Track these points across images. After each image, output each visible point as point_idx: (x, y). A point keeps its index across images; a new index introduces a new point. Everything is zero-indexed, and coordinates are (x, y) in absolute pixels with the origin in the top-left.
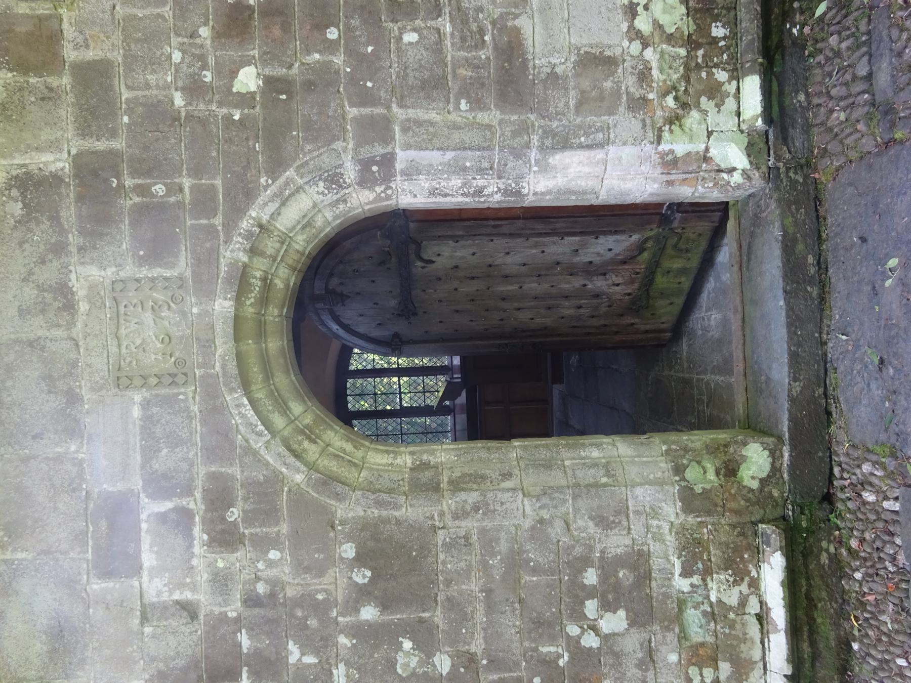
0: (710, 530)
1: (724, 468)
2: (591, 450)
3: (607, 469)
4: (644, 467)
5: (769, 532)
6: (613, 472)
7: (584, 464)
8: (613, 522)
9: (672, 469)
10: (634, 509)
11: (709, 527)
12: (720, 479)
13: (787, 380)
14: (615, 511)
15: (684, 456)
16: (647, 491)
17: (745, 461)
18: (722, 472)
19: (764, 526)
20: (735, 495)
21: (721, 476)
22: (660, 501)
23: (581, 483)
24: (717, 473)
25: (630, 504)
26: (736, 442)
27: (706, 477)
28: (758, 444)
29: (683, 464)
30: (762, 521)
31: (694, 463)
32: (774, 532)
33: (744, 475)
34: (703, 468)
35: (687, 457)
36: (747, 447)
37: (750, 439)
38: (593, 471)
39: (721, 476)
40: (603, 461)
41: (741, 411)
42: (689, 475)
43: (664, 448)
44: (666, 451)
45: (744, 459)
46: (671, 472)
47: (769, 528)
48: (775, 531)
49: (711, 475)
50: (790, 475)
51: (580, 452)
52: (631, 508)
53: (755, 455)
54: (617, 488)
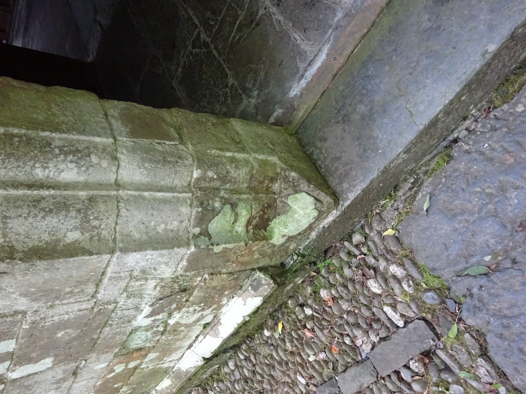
0: (205, 279)
1: (259, 217)
2: (62, 166)
3: (86, 216)
4: (155, 213)
5: (263, 282)
6: (96, 223)
7: (37, 202)
8: (71, 292)
9: (196, 217)
10: (114, 275)
11: (206, 276)
12: (248, 232)
13: (400, 150)
14: (78, 282)
15: (218, 189)
16: (146, 256)
17: (285, 212)
18: (254, 222)
19: (262, 275)
20: (254, 251)
21: (251, 227)
22: (159, 263)
23: (19, 247)
24: (249, 223)
25: (109, 270)
26: (286, 179)
27: (233, 227)
28: (312, 200)
29: (213, 209)
30: (260, 269)
31: (228, 208)
32: (269, 284)
33: (276, 230)
34: (237, 215)
35: (222, 193)
36: (297, 195)
37: (304, 185)
38: (52, 221)
39: (251, 227)
40: (83, 194)
41: (300, 114)
42: (215, 225)
43: (196, 174)
44: (198, 179)
45: (286, 209)
46: (192, 221)
47: (265, 280)
48: (270, 284)
49: (240, 228)
50: (319, 236)
51: (33, 167)
52: (109, 274)
53: (302, 212)
54: (95, 256)
